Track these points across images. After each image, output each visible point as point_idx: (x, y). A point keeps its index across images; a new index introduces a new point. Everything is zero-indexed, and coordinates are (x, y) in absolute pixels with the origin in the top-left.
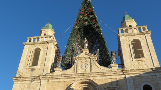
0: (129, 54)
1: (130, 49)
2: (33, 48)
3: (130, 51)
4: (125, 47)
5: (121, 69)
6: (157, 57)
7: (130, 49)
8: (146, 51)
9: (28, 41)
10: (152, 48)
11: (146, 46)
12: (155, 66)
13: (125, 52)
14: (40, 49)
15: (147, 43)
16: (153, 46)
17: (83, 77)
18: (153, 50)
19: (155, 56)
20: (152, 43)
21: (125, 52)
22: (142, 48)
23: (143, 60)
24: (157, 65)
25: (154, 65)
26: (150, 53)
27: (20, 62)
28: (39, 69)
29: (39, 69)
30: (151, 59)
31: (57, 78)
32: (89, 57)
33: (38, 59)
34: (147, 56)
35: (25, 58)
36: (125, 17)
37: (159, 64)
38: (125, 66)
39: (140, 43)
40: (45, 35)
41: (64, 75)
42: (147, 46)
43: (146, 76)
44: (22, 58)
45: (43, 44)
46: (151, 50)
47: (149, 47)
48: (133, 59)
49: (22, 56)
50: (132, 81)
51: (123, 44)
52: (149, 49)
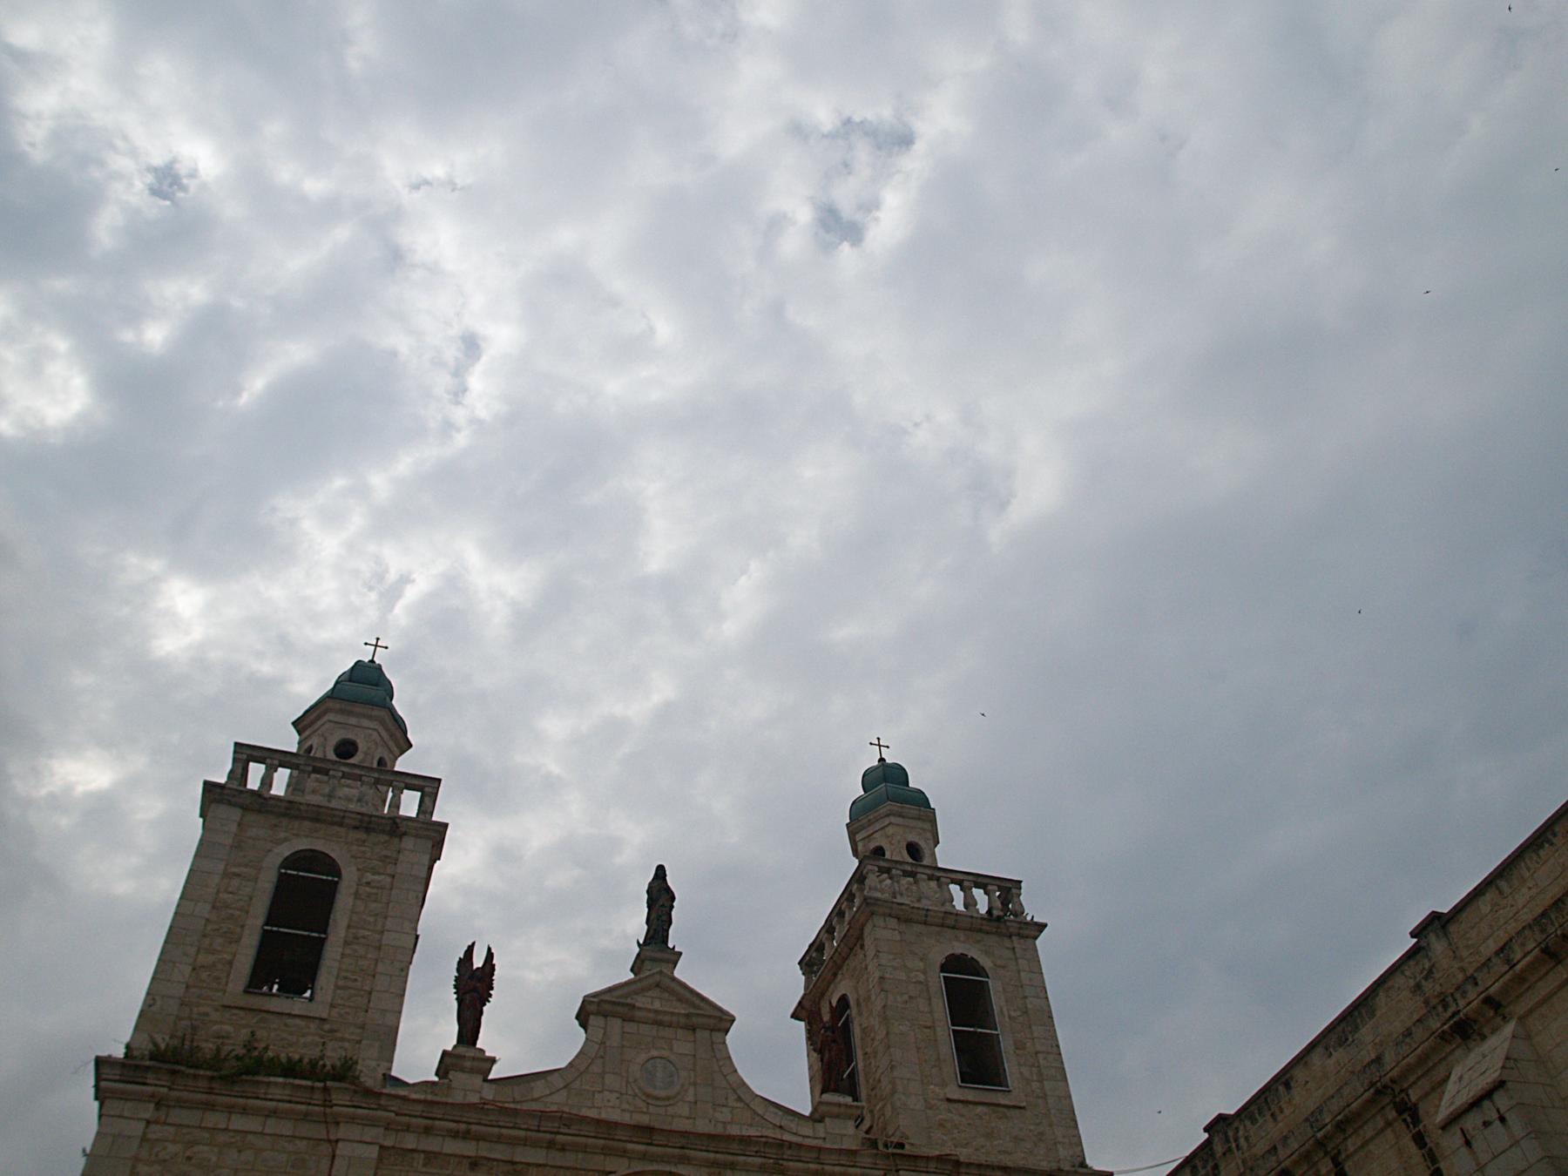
2: (278, 842)
11: (1013, 1014)
14: (338, 873)
17: (644, 1157)
22: (996, 1030)
23: (1003, 1102)
24: (1071, 1153)
29: (327, 1027)
31: (463, 1127)
32: (688, 1016)
41: (515, 1112)
45: (361, 835)
51: (895, 968)
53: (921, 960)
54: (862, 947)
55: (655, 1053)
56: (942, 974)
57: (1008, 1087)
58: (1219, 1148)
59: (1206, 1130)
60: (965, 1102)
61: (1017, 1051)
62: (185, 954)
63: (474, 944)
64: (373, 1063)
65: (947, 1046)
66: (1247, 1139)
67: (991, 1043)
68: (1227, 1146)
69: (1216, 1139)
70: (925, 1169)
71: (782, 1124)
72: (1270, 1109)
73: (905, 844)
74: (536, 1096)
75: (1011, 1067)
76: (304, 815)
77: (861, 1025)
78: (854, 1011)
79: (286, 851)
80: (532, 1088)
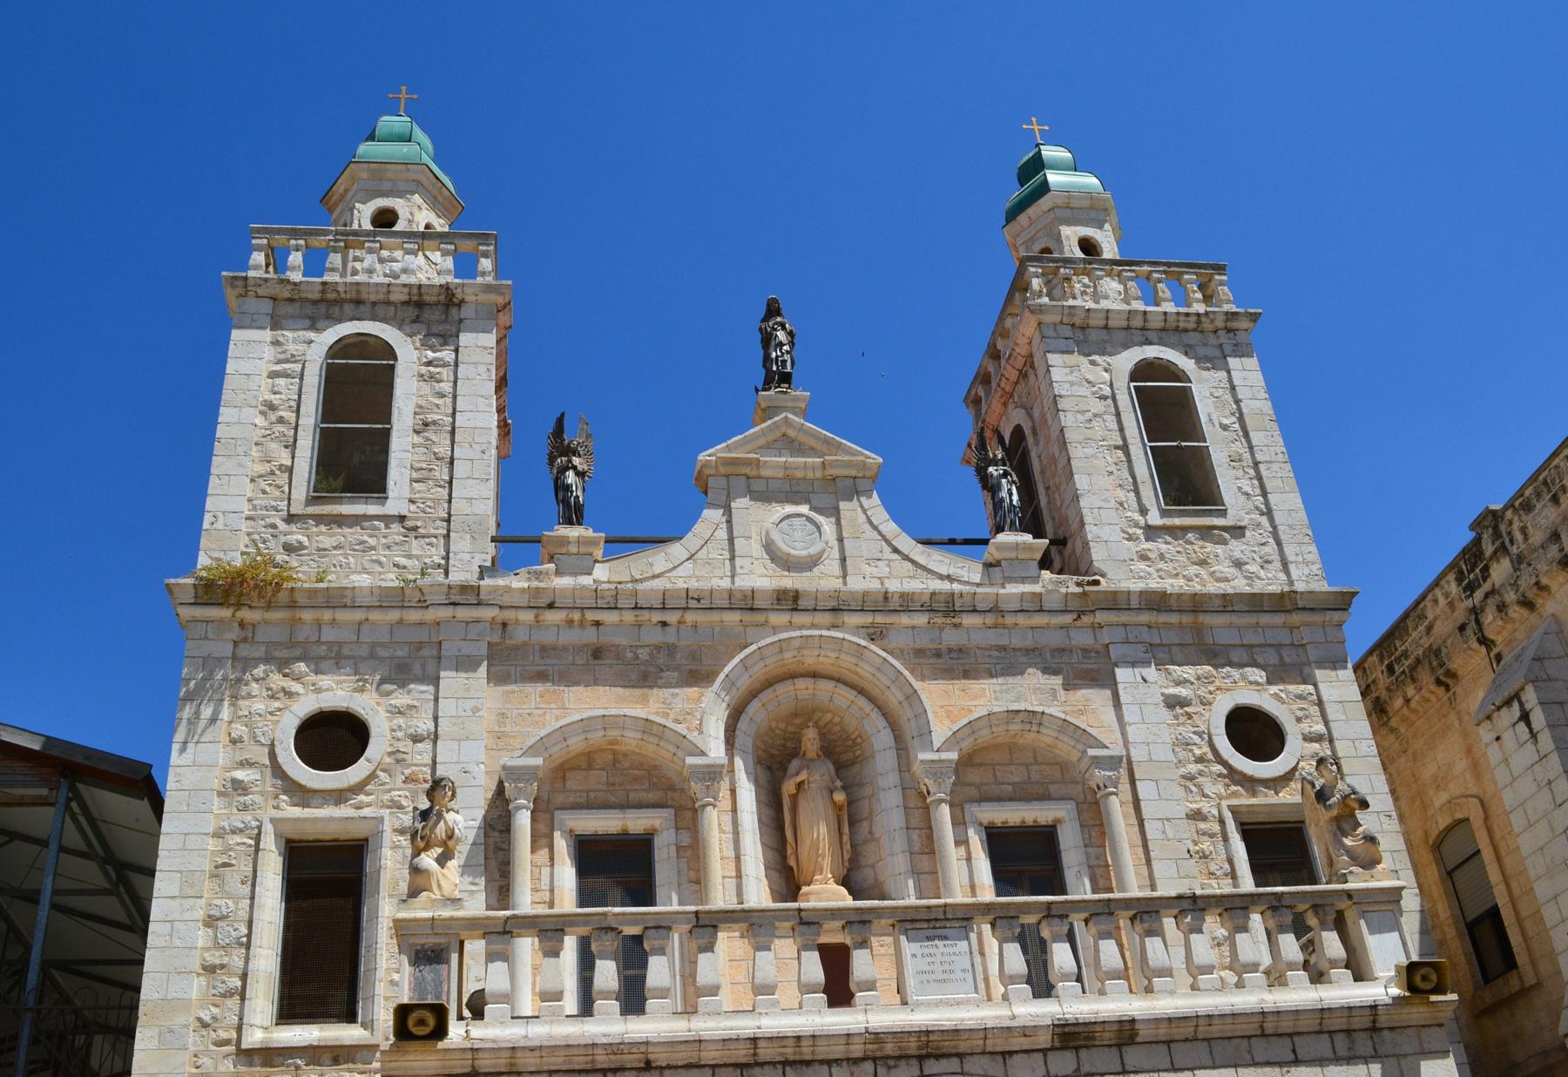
0: (1112, 468)
1: (1121, 429)
3: (1125, 448)
4: (1089, 415)
6: (1302, 515)
7: (1121, 429)
8: (1235, 459)
9: (258, 258)
10: (1269, 441)
11: (1225, 421)
12: (1295, 573)
13: (1089, 451)
14: (390, 352)
15: (1237, 402)
16: (1275, 426)
18: (1280, 458)
19: (1289, 503)
20: (1267, 407)
21: (1089, 451)
24: (1306, 571)
25: (1292, 568)
26: (1260, 479)
27: (218, 448)
28: (409, 524)
33: (387, 434)
35: (259, 421)
38: (1098, 555)
40: (385, 219)
43: (1242, 645)
44: (225, 414)
46: (1268, 459)
47: (1251, 434)
48: (1143, 511)
49: (227, 395)
51: (1072, 384)
52: (1251, 448)
53: (1106, 370)
54: (1032, 366)
56: (1132, 384)
57: (1224, 505)
58: (1488, 548)
59: (1472, 528)
61: (1232, 463)
62: (240, 465)
63: (563, 415)
64: (467, 557)
65: (1143, 467)
66: (1523, 530)
67: (1202, 456)
68: (1497, 543)
69: (1485, 536)
70: (1127, 607)
71: (951, 573)
72: (1549, 491)
73: (1077, 239)
74: (657, 571)
75: (1231, 483)
76: (343, 296)
77: (1039, 457)
78: (1030, 440)
80: (651, 565)
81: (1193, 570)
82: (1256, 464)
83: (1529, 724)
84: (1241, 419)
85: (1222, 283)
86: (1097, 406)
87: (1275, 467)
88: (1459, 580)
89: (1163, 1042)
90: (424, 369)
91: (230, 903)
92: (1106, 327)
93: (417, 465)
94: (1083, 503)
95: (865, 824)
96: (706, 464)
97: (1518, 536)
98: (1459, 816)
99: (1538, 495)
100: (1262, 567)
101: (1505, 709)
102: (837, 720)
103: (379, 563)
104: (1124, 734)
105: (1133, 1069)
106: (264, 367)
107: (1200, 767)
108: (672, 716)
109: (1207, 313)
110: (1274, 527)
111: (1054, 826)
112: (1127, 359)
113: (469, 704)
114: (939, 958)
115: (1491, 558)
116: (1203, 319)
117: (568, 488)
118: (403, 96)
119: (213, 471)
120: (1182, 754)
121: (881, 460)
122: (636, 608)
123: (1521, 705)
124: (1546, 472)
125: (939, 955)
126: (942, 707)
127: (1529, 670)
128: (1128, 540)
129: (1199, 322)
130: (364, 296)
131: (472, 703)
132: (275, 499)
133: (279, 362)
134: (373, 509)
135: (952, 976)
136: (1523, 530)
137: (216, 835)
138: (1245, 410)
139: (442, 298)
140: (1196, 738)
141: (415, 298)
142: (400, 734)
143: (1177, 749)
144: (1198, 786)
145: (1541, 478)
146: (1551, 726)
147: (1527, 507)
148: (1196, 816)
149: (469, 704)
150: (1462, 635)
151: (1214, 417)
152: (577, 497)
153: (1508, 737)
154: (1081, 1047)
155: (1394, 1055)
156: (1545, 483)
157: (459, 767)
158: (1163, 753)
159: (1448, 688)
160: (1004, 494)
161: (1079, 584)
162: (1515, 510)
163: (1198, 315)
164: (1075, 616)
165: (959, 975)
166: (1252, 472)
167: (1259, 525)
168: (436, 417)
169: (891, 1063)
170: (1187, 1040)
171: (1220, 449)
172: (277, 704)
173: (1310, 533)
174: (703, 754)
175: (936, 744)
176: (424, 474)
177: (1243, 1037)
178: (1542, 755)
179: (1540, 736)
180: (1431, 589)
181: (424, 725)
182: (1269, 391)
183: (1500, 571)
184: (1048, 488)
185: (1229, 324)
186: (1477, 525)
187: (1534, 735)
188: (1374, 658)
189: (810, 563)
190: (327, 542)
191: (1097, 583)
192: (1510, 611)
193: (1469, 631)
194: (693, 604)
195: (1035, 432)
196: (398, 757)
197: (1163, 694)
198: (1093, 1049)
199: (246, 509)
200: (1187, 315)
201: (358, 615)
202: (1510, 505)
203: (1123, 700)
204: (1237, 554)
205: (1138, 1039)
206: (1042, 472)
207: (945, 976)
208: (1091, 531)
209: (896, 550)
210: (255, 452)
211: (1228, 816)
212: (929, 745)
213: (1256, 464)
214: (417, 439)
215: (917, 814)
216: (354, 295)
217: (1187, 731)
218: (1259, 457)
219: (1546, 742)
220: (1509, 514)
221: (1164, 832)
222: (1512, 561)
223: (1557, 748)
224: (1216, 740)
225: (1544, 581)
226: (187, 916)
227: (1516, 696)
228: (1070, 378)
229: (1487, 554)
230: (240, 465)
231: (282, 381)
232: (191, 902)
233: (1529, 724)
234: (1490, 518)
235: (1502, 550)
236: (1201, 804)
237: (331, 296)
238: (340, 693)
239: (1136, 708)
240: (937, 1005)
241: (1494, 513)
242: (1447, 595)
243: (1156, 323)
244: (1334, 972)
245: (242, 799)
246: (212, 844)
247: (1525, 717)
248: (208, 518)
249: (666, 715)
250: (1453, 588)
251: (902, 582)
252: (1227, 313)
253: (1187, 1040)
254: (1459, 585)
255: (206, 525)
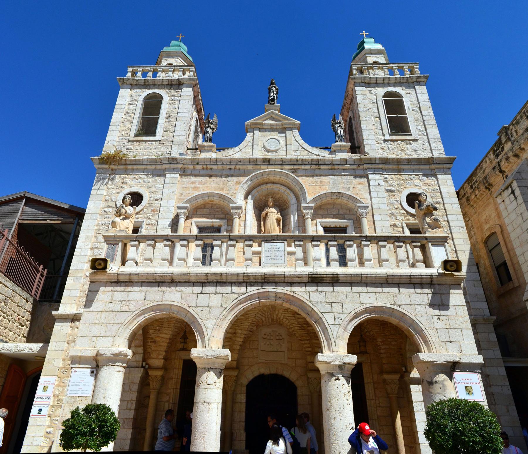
0: (375, 123)
2: (143, 92)
3: (379, 117)
4: (368, 108)
5: (357, 156)
6: (439, 136)
7: (379, 112)
9: (129, 75)
10: (429, 114)
11: (414, 109)
13: (367, 118)
14: (162, 98)
15: (419, 103)
16: (431, 109)
18: (432, 118)
19: (434, 132)
20: (429, 104)
21: (367, 118)
24: (438, 152)
25: (433, 151)
26: (425, 125)
28: (161, 142)
30: (425, 138)
33: (158, 119)
34: (418, 132)
35: (124, 116)
36: (363, 42)
37: (442, 151)
38: (367, 148)
39: (402, 100)
42: (418, 110)
44: (114, 115)
47: (423, 112)
48: (384, 135)
49: (115, 110)
50: (382, 182)
51: (363, 99)
52: (422, 116)
53: (375, 95)
55: (271, 137)
58: (503, 140)
60: (393, 141)
62: (117, 128)
66: (516, 132)
67: (405, 119)
68: (507, 138)
69: (503, 136)
74: (230, 155)
76: (150, 83)
79: (145, 94)
81: (399, 152)
82: (424, 121)
83: (514, 195)
84: (420, 108)
85: (417, 68)
86: (371, 106)
87: (430, 121)
88: (494, 153)
89: (349, 283)
90: (170, 102)
91: (98, 244)
92: (376, 83)
93: (165, 127)
94: (363, 133)
95: (288, 226)
96: (248, 125)
97: (514, 134)
98: (493, 231)
99: (522, 118)
100: (423, 151)
101: (506, 191)
102: (281, 196)
103: (152, 153)
104: (371, 200)
105: (337, 291)
106: (126, 103)
107: (396, 211)
108: (230, 194)
109: (410, 77)
110: (428, 139)
111: (346, 228)
112: (382, 91)
113: (172, 190)
114: (274, 252)
115: (504, 143)
116: (409, 79)
117: (207, 132)
118: (181, 36)
119: (109, 130)
120: (390, 207)
121: (300, 122)
122: (222, 164)
123: (512, 188)
124: (525, 109)
125: (274, 252)
126: (313, 192)
127: (515, 176)
128: (378, 144)
129: (407, 80)
130: (156, 83)
131: (173, 190)
132: (125, 137)
133: (131, 101)
134: (152, 138)
135: (277, 258)
136: (516, 132)
137: (97, 225)
138: (421, 105)
139: (178, 82)
140: (396, 202)
141: (170, 83)
142: (151, 199)
143: (389, 205)
144: (395, 217)
145: (523, 111)
146: (522, 194)
147: (518, 123)
148: (394, 225)
149: (172, 190)
150: (494, 171)
151: (410, 108)
152: (210, 135)
153: (507, 201)
154: (319, 283)
155: (439, 294)
156: (524, 113)
157: (167, 207)
158: (383, 206)
159: (489, 190)
160: (339, 131)
161: (360, 157)
162: (513, 125)
163: (407, 77)
164: (357, 166)
165: (280, 257)
166: (422, 123)
167: (423, 139)
168: (172, 114)
169: (252, 284)
170: (358, 283)
171: (411, 117)
172: (119, 191)
173: (441, 141)
174: (235, 203)
175: (308, 201)
176: (167, 129)
177: (380, 283)
178: (519, 204)
179: (518, 198)
180: (484, 158)
181: (158, 196)
182: (430, 100)
183: (507, 147)
184: (356, 133)
185: (418, 80)
186: (500, 132)
187: (516, 198)
188: (467, 184)
189: (276, 151)
190: (138, 148)
191: (366, 156)
192: (510, 159)
193: (496, 169)
194: (239, 163)
195: (354, 117)
196: (150, 205)
197: (385, 189)
198: (323, 284)
199: (117, 139)
200: (403, 78)
201: (144, 167)
202: (512, 124)
203: (371, 190)
204: (415, 148)
205: (340, 281)
206: (355, 128)
207: (275, 258)
208: (365, 141)
209: (303, 148)
210: (122, 124)
211: (405, 226)
212: (305, 202)
213: (424, 121)
214: (166, 120)
215: (302, 223)
216: (153, 83)
217: (393, 200)
218: (424, 119)
219: (520, 199)
220: (511, 127)
221: (382, 230)
222: (512, 143)
223: (524, 201)
224: (402, 203)
225: (522, 146)
226: (86, 247)
227: (510, 185)
228: (363, 98)
229: (503, 142)
230: (117, 128)
231: (131, 106)
232: (88, 243)
233: (514, 195)
234: (504, 130)
235: (509, 139)
236: (396, 222)
237: (147, 83)
238: (137, 188)
239: (376, 193)
240: (270, 266)
241: (506, 127)
242: (490, 159)
243: (393, 81)
244: (418, 264)
245: (106, 216)
246: (96, 228)
247: (513, 192)
248: (106, 142)
249: (228, 194)
250: (492, 156)
251: (302, 155)
252: (417, 76)
253: (358, 283)
254: (494, 155)
255: (105, 144)
